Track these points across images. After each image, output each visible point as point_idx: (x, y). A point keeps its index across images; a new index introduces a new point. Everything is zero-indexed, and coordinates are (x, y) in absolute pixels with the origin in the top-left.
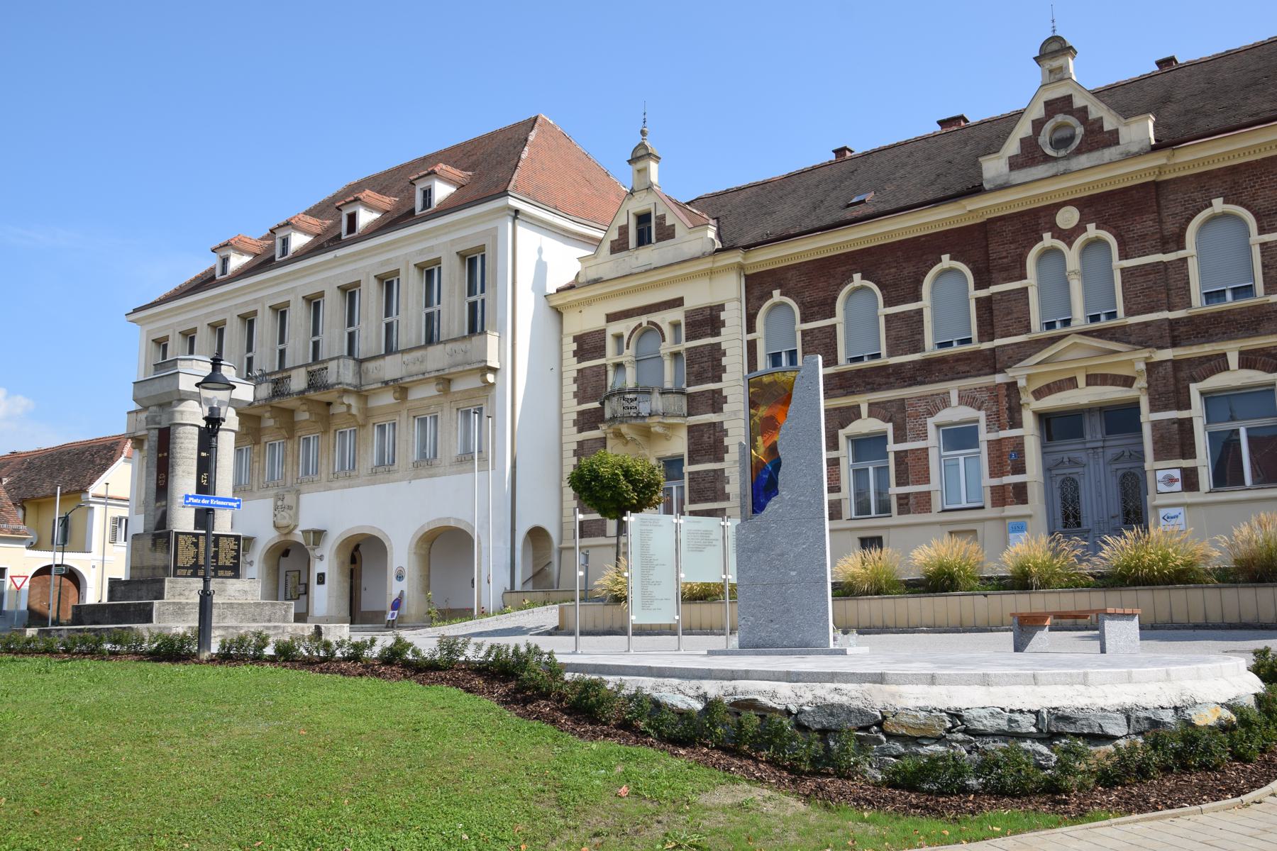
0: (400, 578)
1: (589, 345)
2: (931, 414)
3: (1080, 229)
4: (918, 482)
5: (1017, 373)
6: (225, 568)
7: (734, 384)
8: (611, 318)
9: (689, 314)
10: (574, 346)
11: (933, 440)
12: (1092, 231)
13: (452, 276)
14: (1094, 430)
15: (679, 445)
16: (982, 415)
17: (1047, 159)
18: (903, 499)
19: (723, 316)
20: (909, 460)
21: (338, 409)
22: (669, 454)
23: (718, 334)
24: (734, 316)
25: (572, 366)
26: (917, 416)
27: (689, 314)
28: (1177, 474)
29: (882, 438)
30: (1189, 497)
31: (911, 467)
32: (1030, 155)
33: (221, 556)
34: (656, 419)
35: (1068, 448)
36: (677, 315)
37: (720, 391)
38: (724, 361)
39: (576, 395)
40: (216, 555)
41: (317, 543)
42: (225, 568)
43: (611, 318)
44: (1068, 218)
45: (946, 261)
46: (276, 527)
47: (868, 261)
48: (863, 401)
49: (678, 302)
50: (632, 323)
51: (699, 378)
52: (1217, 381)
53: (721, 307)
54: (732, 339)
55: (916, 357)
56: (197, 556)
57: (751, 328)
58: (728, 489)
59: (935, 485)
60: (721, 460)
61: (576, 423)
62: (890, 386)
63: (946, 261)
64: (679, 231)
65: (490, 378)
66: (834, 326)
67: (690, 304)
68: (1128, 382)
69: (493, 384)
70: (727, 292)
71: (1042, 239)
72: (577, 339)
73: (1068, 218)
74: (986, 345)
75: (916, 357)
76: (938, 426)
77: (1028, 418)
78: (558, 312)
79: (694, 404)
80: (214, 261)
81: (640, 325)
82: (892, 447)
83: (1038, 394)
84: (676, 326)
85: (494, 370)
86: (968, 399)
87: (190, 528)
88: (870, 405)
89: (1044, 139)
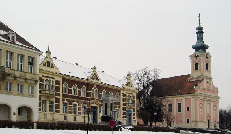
0: (14, 114)
4: (80, 111)
12: (97, 89)
18: (78, 112)
19: (60, 83)
22: (52, 100)
24: (61, 83)
29: (76, 105)
37: (59, 93)
44: (95, 86)
45: (84, 86)
48: (75, 100)
50: (46, 78)
53: (60, 82)
57: (62, 86)
62: (78, 99)
63: (84, 86)
68: (98, 105)
79: (56, 94)
81: (48, 79)
83: (92, 104)
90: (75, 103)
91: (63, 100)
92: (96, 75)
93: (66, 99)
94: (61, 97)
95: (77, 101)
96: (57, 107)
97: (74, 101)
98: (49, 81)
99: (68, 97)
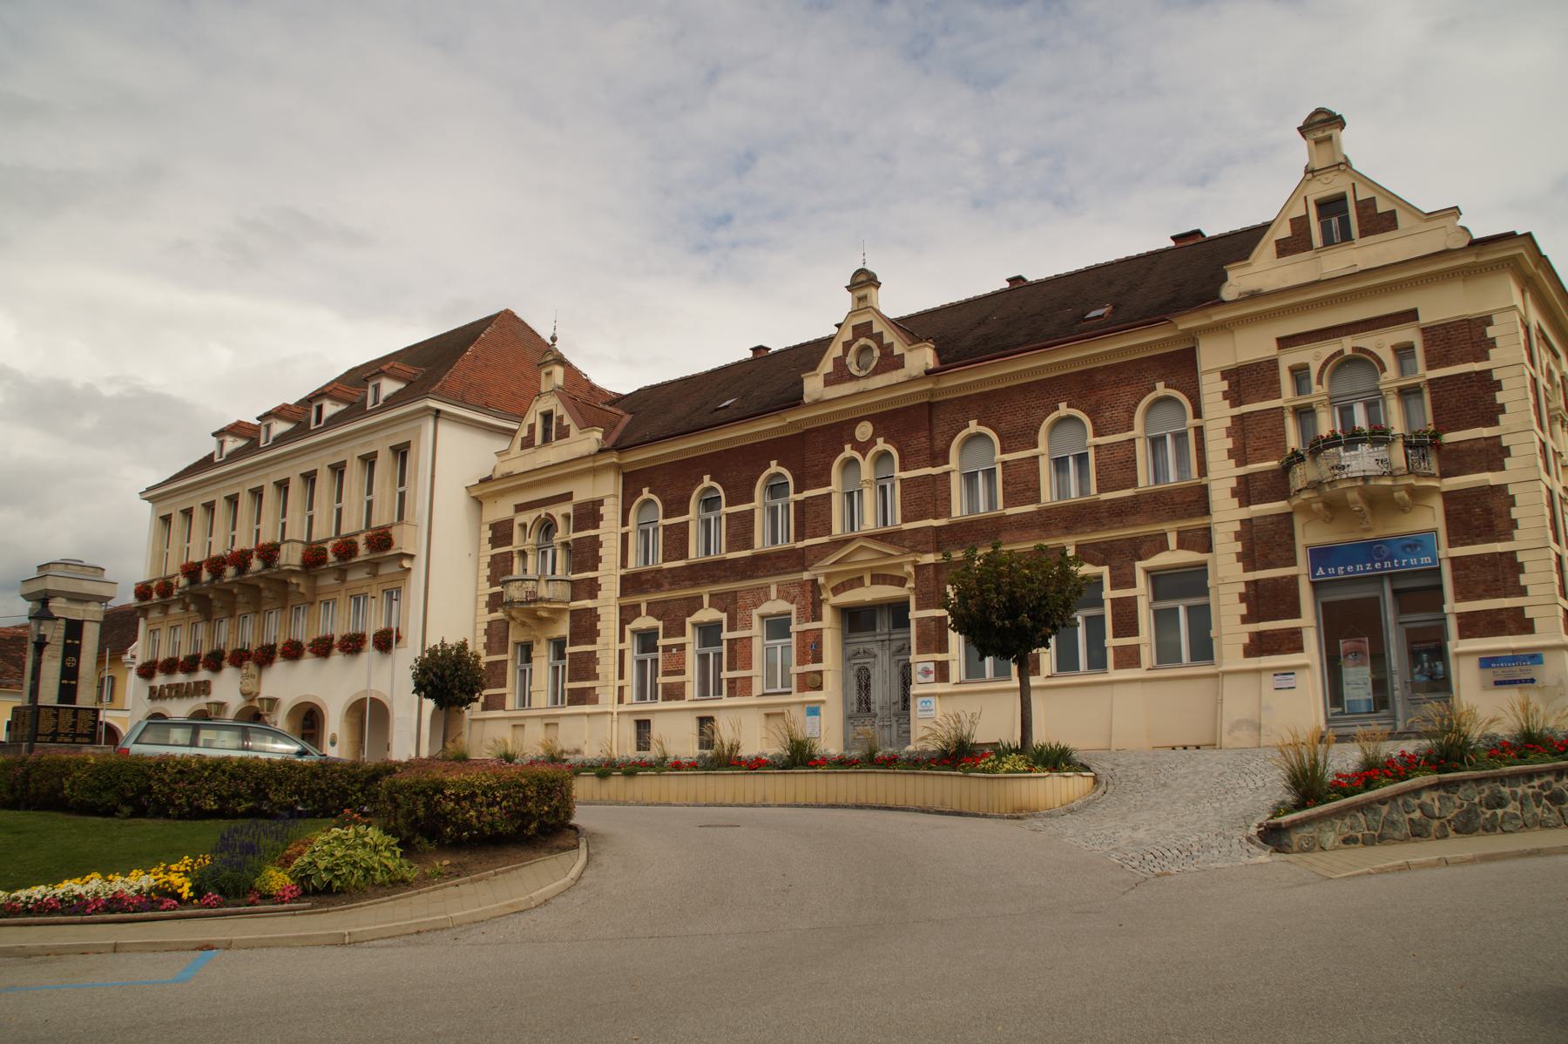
0: (333, 743)
1: (501, 533)
2: (756, 606)
3: (872, 442)
4: (743, 668)
5: (816, 572)
6: (83, 735)
7: (609, 574)
8: (520, 508)
9: (578, 507)
10: (490, 534)
11: (757, 630)
12: (881, 445)
13: (384, 464)
14: (883, 624)
15: (563, 629)
16: (793, 608)
17: (852, 378)
18: (732, 681)
20: (738, 647)
21: (292, 588)
23: (597, 527)
24: (611, 511)
25: (488, 551)
26: (746, 608)
27: (578, 507)
28: (931, 667)
29: (716, 626)
30: (940, 688)
31: (739, 653)
32: (840, 374)
33: (80, 725)
34: (539, 605)
35: (863, 641)
36: (568, 508)
38: (601, 552)
39: (489, 579)
40: (74, 725)
41: (270, 709)
42: (83, 735)
43: (520, 508)
44: (864, 431)
46: (244, 694)
47: (715, 463)
48: (705, 593)
49: (568, 497)
51: (577, 566)
52: (1160, 560)
53: (600, 502)
54: (609, 531)
55: (747, 553)
56: (56, 725)
57: (625, 523)
58: (599, 669)
59: (757, 670)
60: (594, 642)
61: (488, 604)
62: (727, 579)
64: (574, 430)
65: (406, 564)
66: (687, 522)
67: (577, 498)
68: (901, 582)
69: (409, 569)
70: (607, 489)
71: (1057, 409)
72: (493, 527)
73: (864, 431)
74: (800, 545)
75: (747, 553)
76: (762, 617)
77: (827, 611)
78: (478, 501)
80: (211, 446)
82: (725, 635)
83: (836, 591)
84: (567, 517)
85: (411, 557)
86: (784, 595)
87: (54, 702)
88: (711, 596)
89: (851, 359)
90: (707, 614)
91: (627, 614)
92: (871, 336)
93: (643, 600)
94: (608, 603)
95: (717, 601)
96: (585, 667)
97: (694, 604)
98: (1364, 361)
99: (658, 587)
